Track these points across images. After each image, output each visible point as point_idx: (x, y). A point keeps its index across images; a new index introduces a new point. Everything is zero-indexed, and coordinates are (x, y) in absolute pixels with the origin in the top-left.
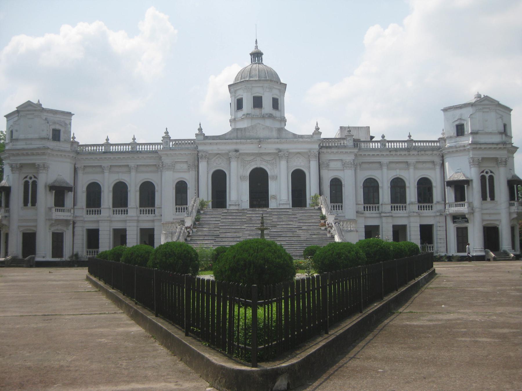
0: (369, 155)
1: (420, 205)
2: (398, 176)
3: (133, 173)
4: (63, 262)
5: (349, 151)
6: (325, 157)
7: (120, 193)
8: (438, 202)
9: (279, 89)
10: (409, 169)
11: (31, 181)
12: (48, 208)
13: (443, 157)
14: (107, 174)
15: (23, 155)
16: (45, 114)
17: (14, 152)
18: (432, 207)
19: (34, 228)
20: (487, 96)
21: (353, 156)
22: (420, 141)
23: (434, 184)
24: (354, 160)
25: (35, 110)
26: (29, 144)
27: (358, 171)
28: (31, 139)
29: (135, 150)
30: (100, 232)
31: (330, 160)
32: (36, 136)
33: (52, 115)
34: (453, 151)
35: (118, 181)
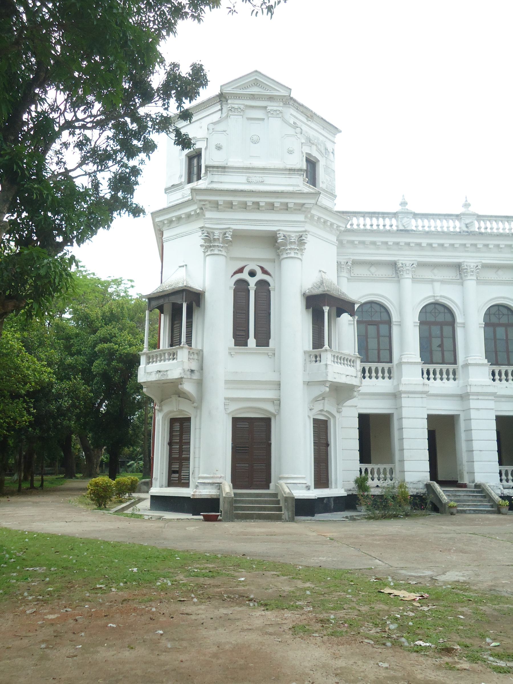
3: (471, 284)
4: (337, 499)
7: (438, 326)
11: (252, 282)
12: (305, 352)
14: (407, 283)
15: (244, 207)
16: (292, 111)
17: (221, 199)
19: (270, 408)
25: (271, 98)
26: (257, 183)
28: (264, 170)
29: (472, 229)
30: (405, 423)
32: (276, 163)
33: (304, 119)
35: (432, 300)
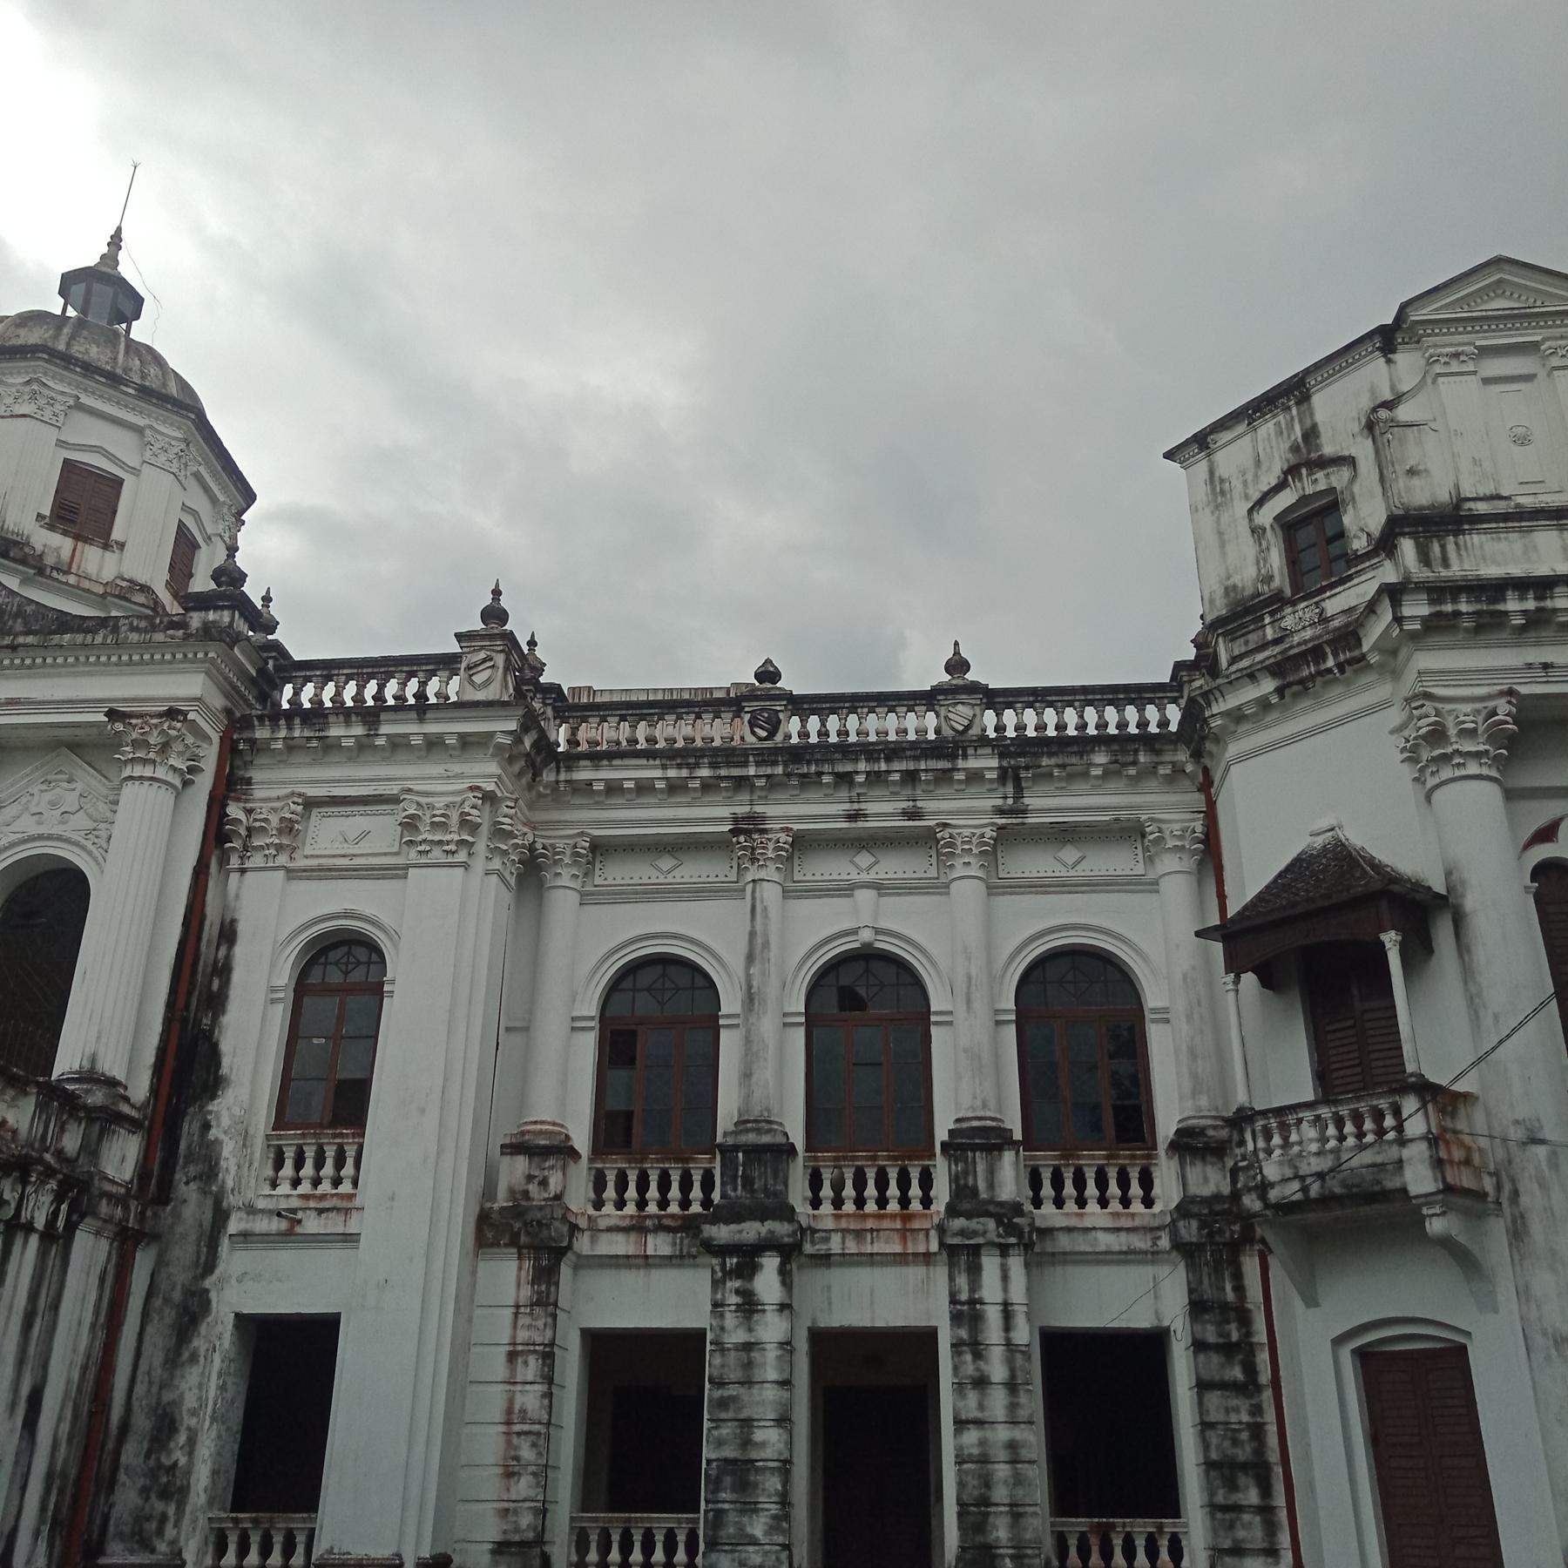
0: (644, 788)
1: (1047, 1161)
2: (866, 936)
5: (450, 728)
6: (274, 785)
8: (1189, 1144)
9: (139, 431)
10: (943, 888)
13: (1206, 785)
18: (1147, 1182)
20: (1499, 262)
21: (493, 768)
22: (1039, 697)
23: (1153, 997)
24: (489, 798)
27: (563, 899)
31: (310, 804)
34: (1264, 704)
